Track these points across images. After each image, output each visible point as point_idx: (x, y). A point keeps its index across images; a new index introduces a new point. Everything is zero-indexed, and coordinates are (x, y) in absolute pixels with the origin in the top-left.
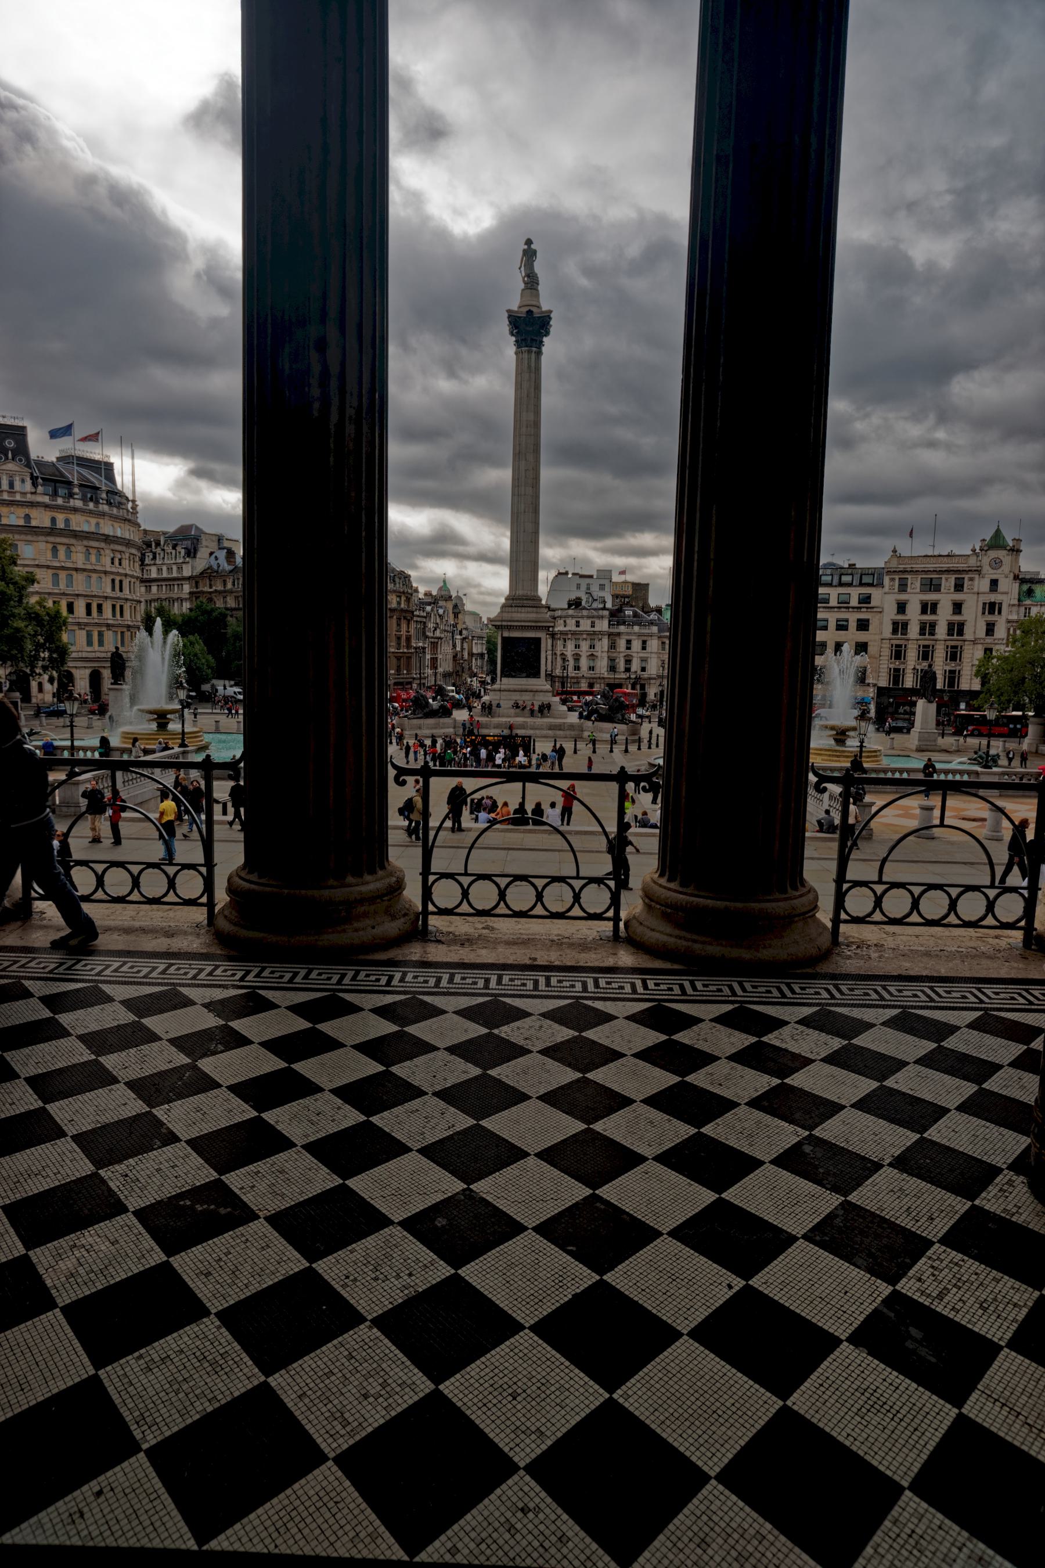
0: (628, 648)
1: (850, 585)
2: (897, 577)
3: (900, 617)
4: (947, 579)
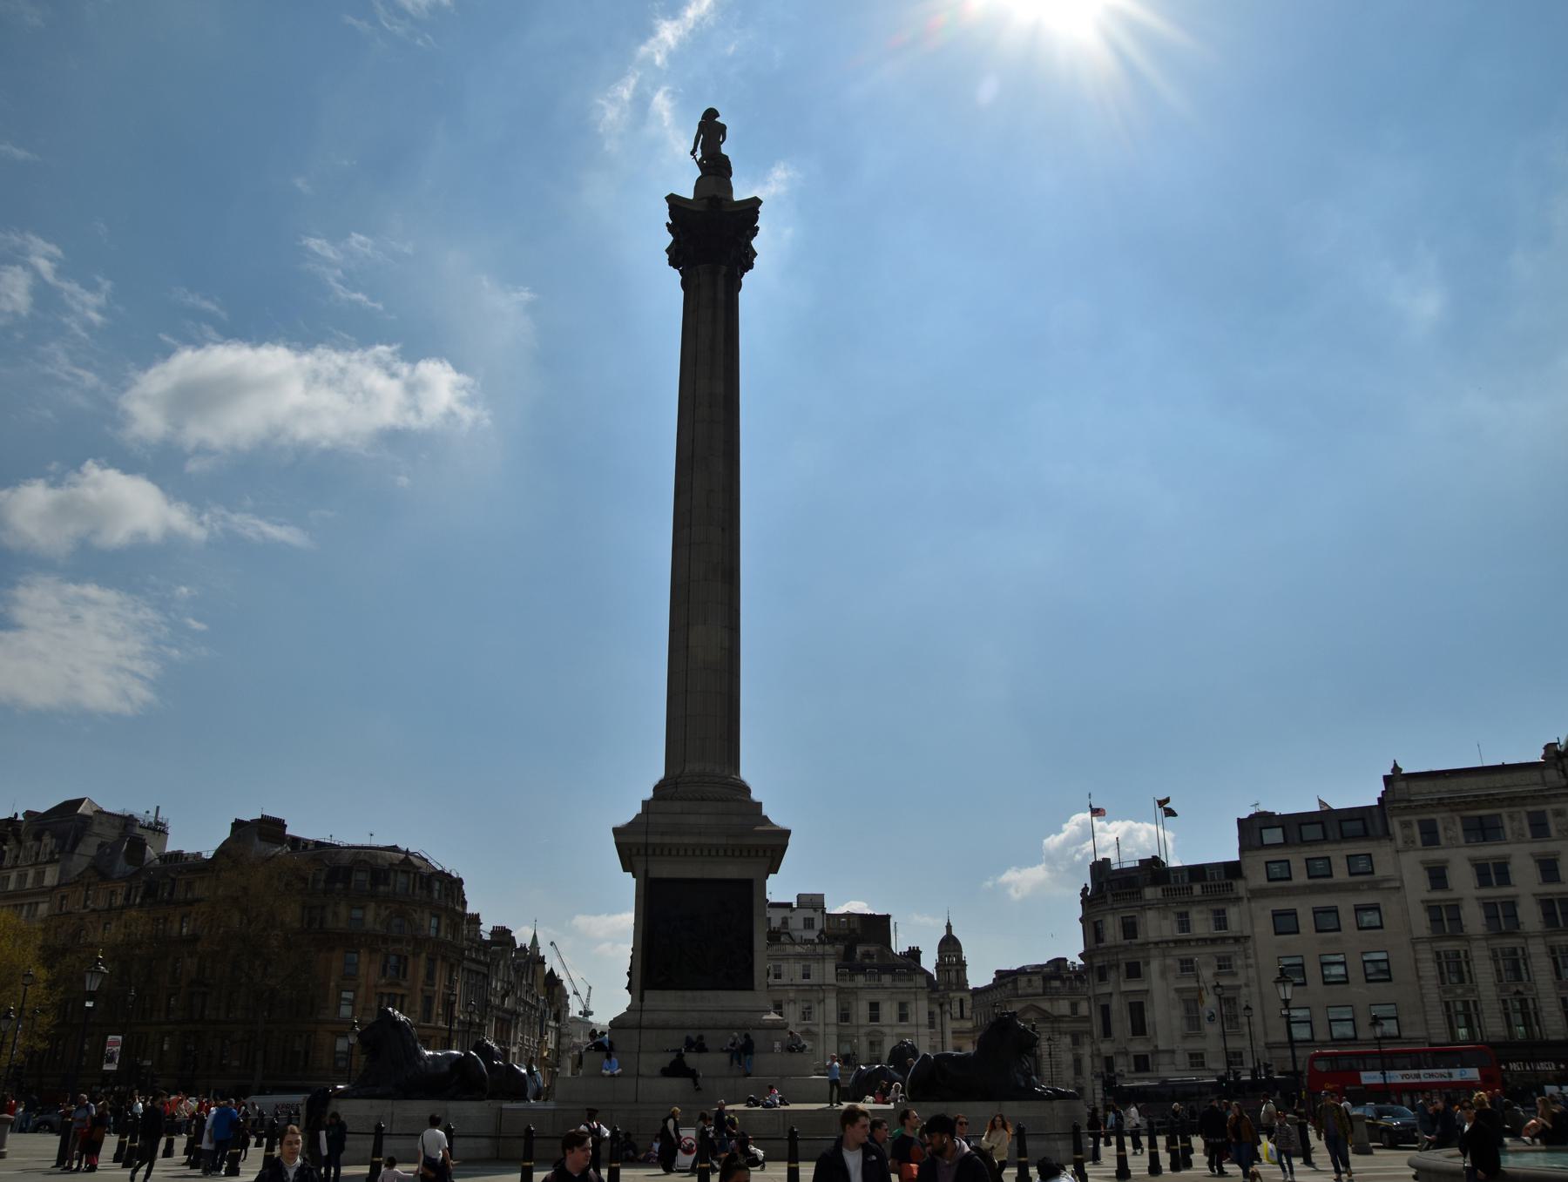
0: (874, 1017)
1: (1326, 839)
2: (1414, 818)
3: (1438, 895)
4: (1511, 817)
